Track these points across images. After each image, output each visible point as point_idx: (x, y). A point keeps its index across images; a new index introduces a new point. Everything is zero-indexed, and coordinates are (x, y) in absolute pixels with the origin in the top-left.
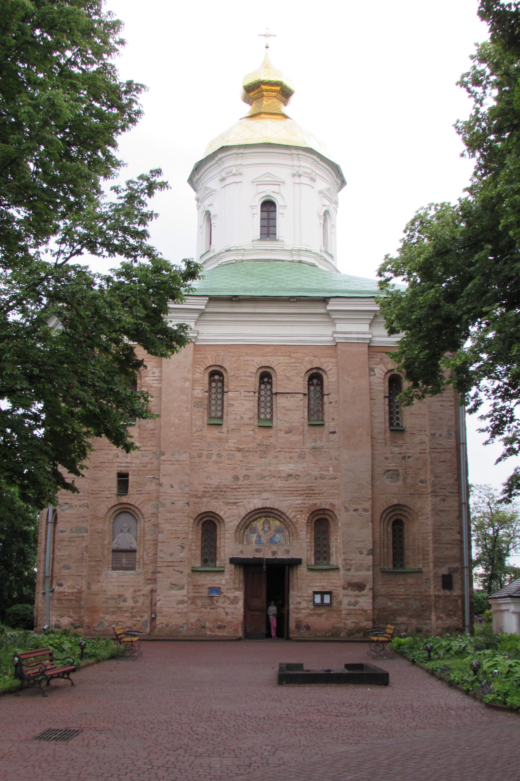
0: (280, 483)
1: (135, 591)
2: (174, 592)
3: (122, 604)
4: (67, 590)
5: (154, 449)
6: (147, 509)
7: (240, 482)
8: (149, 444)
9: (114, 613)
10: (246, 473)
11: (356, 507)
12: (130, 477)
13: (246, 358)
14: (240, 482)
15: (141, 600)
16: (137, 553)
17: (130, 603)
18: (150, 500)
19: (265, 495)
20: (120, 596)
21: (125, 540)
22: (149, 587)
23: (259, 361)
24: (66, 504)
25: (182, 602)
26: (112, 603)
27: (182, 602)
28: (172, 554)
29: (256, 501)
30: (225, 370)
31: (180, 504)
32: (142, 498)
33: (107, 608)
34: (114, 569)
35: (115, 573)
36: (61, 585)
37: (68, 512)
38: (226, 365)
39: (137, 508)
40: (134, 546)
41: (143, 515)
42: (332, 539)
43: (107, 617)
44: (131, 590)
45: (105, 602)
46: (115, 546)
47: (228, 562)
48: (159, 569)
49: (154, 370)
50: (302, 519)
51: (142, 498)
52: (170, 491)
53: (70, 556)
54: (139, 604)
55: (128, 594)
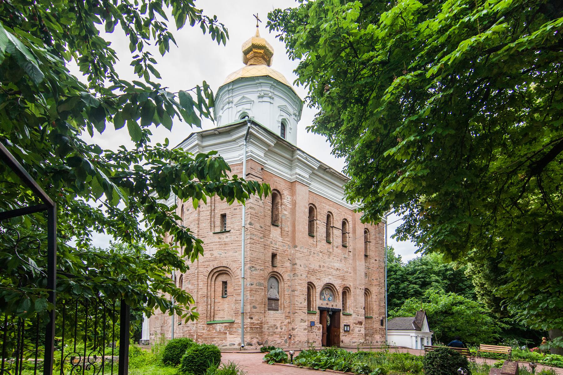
0: (335, 272)
1: (281, 323)
2: (302, 324)
3: (276, 330)
4: (255, 322)
5: (288, 243)
6: (286, 277)
7: (321, 269)
8: (286, 239)
9: (272, 335)
10: (323, 264)
11: (360, 287)
12: (278, 257)
13: (324, 205)
14: (321, 269)
15: (284, 327)
16: (280, 301)
17: (279, 330)
18: (287, 272)
19: (330, 277)
20: (275, 325)
21: (273, 293)
22: (287, 321)
23: (328, 208)
24: (253, 267)
25: (305, 329)
26: (271, 329)
27: (305, 329)
28: (301, 303)
29: (327, 279)
30: (316, 208)
31: (304, 276)
32: (284, 270)
33: (269, 332)
34: (269, 310)
35: (272, 312)
36: (252, 318)
37: (254, 272)
38: (316, 205)
39: (281, 275)
40: (278, 297)
41: (283, 280)
42: (348, 301)
43: (270, 338)
44: (280, 322)
45: (268, 329)
46: (269, 296)
47: (317, 309)
48: (296, 311)
49: (288, 196)
50: (340, 291)
51: (284, 270)
52: (300, 268)
53: (256, 300)
54: (283, 330)
55: (278, 325)
